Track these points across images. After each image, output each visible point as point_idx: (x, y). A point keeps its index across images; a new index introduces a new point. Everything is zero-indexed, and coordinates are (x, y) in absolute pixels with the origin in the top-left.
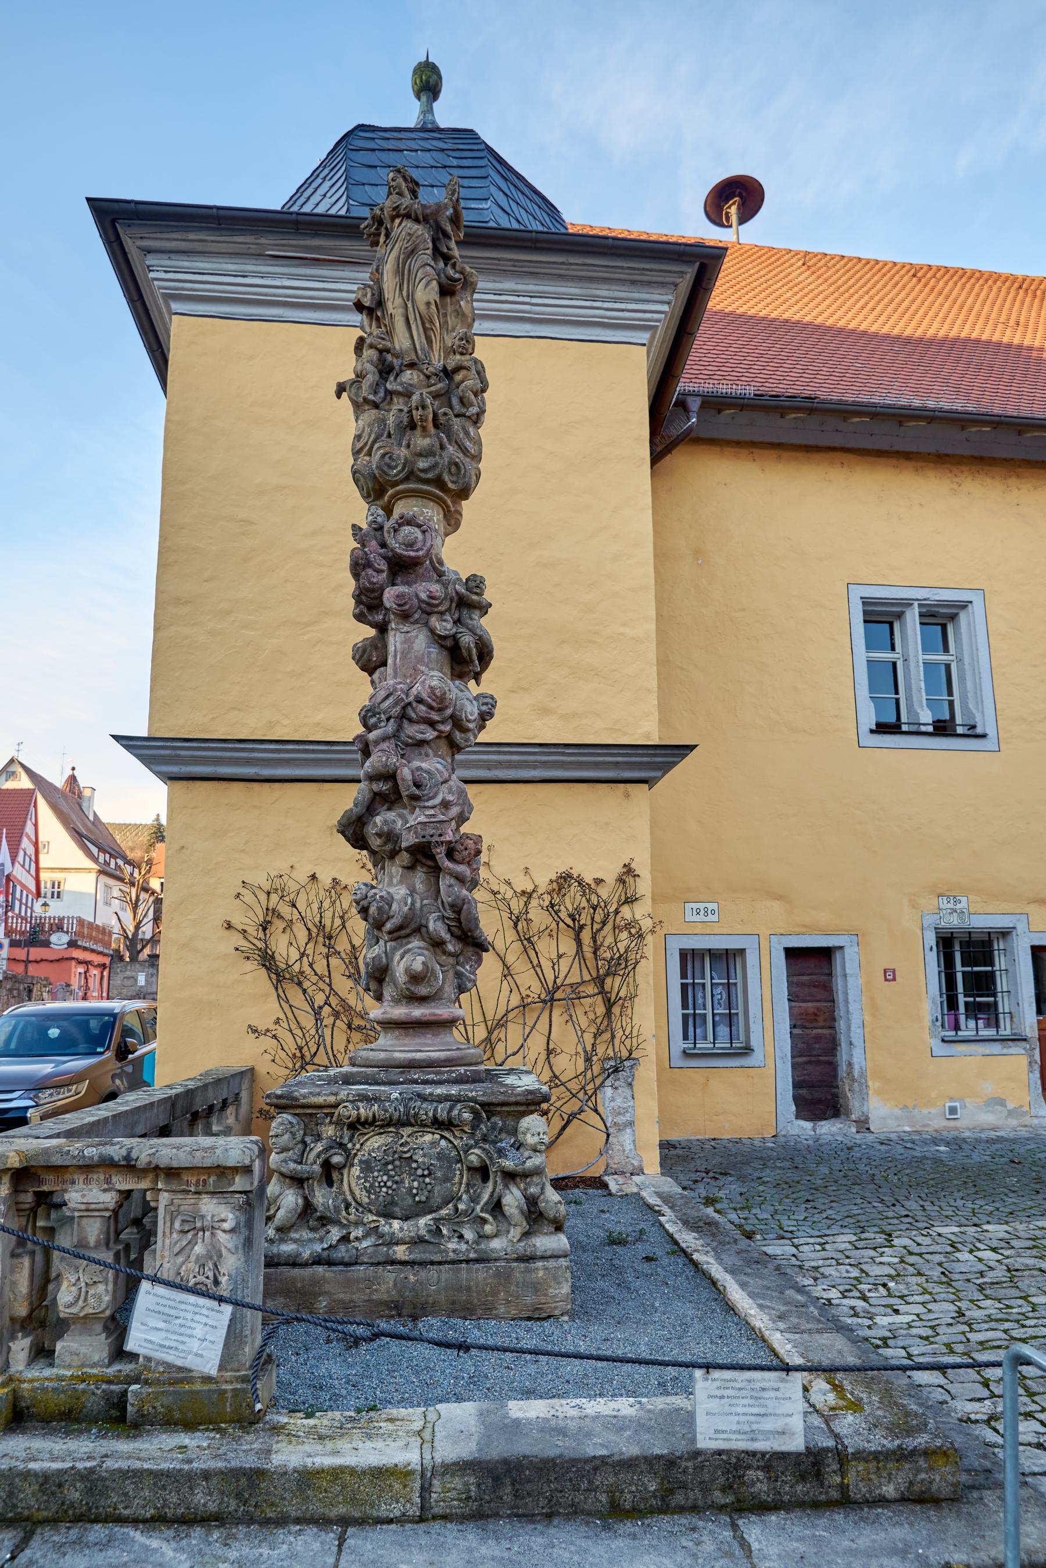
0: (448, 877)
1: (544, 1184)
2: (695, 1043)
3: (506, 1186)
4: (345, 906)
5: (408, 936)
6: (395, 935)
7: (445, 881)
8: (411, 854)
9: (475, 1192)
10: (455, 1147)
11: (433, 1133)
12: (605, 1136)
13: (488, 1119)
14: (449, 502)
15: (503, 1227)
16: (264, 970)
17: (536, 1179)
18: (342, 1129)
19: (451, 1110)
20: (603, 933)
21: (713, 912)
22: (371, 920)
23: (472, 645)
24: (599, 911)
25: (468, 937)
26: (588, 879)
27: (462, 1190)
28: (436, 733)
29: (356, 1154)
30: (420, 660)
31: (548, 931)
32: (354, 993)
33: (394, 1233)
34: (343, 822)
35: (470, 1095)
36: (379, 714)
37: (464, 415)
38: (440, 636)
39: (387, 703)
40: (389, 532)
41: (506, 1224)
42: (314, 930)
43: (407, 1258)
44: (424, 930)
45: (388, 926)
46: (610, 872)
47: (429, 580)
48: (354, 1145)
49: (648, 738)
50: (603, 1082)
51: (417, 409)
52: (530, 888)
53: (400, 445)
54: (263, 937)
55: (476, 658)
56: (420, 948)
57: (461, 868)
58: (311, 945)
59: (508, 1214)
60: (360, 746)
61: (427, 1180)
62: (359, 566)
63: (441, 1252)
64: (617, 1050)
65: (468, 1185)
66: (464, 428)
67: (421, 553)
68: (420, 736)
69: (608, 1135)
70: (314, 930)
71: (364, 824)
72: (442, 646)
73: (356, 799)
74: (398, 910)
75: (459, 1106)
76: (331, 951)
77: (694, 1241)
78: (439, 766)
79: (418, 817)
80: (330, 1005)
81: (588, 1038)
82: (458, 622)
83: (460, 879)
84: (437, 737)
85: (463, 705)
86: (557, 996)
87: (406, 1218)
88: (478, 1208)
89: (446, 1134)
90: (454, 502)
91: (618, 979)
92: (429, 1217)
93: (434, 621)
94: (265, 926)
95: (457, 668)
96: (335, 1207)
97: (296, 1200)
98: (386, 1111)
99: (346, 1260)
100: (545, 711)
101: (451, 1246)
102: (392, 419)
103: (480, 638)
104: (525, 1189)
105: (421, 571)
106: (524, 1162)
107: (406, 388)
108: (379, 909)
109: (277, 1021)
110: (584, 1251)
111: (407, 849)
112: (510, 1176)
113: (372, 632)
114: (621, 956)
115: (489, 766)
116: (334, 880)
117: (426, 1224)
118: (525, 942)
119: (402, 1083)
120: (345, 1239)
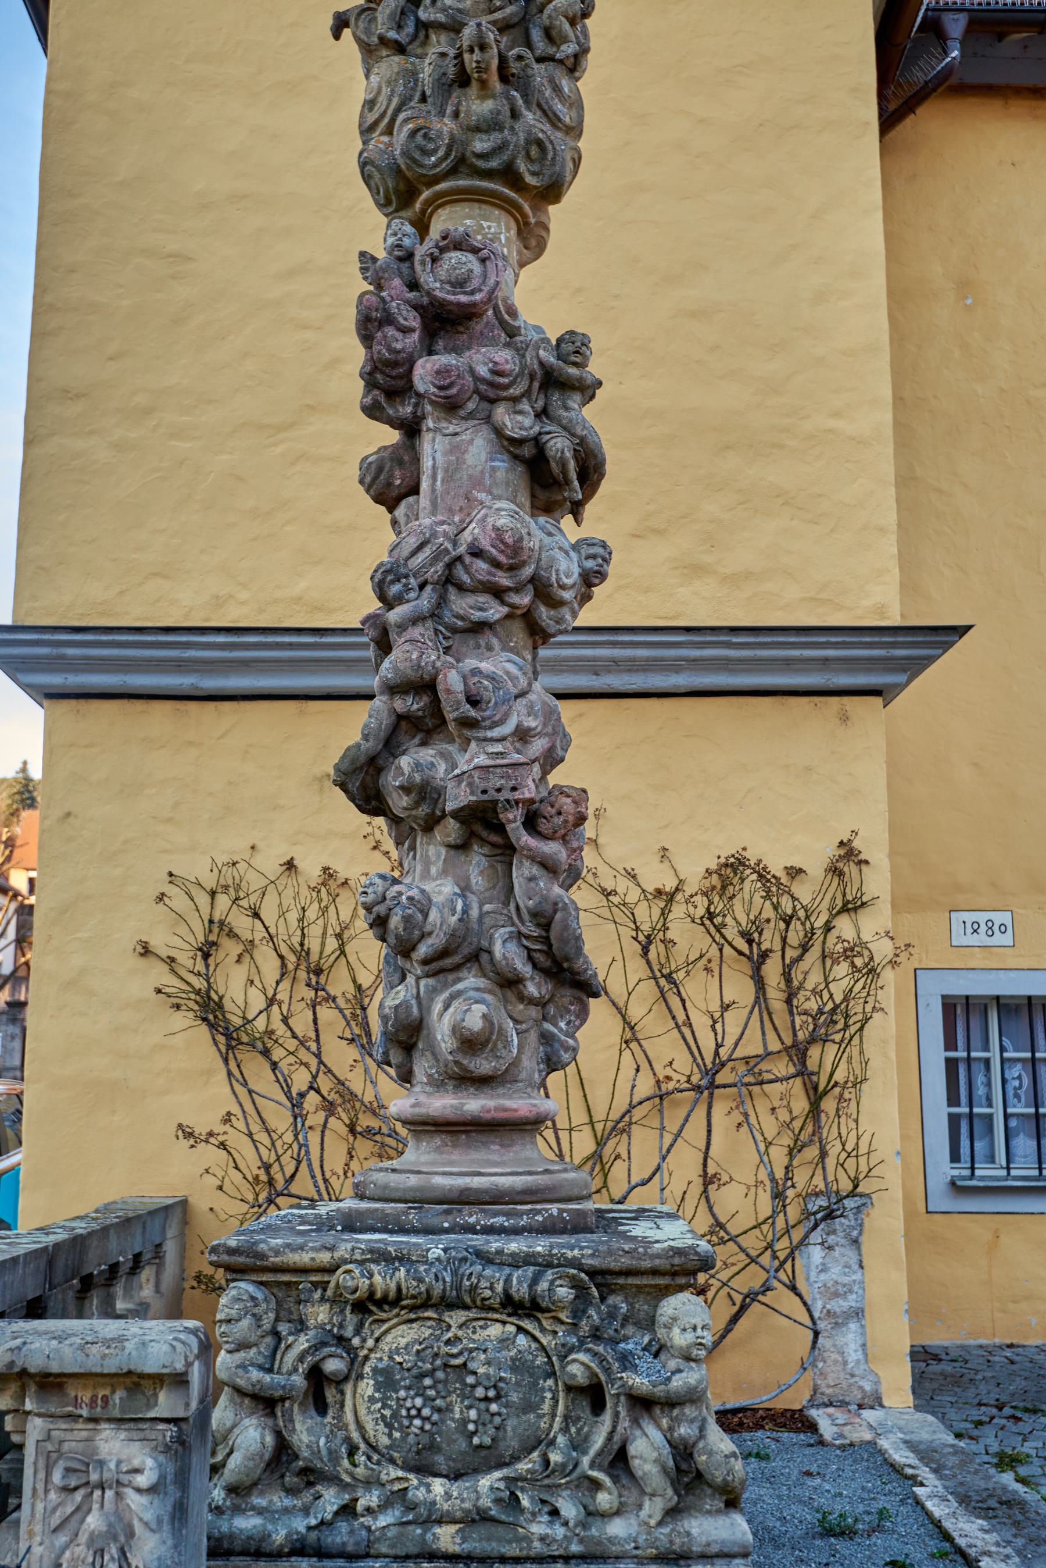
0: (527, 863)
1: (704, 1420)
2: (973, 1168)
3: (636, 1422)
4: (345, 915)
5: (457, 967)
6: (435, 966)
7: (522, 871)
8: (462, 823)
9: (579, 1431)
10: (543, 1348)
11: (504, 1323)
12: (810, 1335)
13: (603, 1299)
14: (527, 208)
15: (631, 1497)
16: (204, 1028)
17: (689, 1411)
18: (342, 1311)
19: (535, 1281)
20: (803, 965)
21: (1003, 929)
22: (392, 940)
23: (568, 454)
24: (795, 924)
25: (562, 970)
26: (776, 868)
27: (556, 1426)
28: (505, 610)
29: (366, 1358)
30: (477, 483)
31: (704, 961)
32: (359, 1069)
33: (434, 1503)
34: (344, 767)
35: (570, 1254)
36: (407, 577)
37: (551, 59)
38: (512, 441)
39: (420, 558)
40: (423, 263)
41: (635, 1492)
42: (291, 959)
43: (457, 1549)
44: (484, 957)
45: (423, 950)
46: (815, 855)
47: (494, 342)
48: (364, 1340)
49: (882, 615)
50: (806, 1236)
51: (471, 50)
52: (670, 885)
53: (442, 113)
54: (203, 971)
55: (573, 476)
56: (477, 989)
58: (285, 985)
59: (639, 1473)
60: (373, 633)
61: (494, 1407)
62: (371, 323)
63: (519, 1539)
64: (831, 1178)
65: (566, 1418)
66: (552, 81)
67: (478, 297)
68: (477, 615)
69: (816, 1334)
70: (291, 959)
71: (380, 770)
72: (516, 457)
73: (366, 726)
74: (440, 922)
75: (549, 1275)
76: (321, 996)
77: (980, 1534)
78: (510, 667)
79: (475, 756)
80: (318, 1091)
81: (779, 1156)
82: (543, 414)
83: (548, 866)
84: (508, 616)
85: (553, 559)
86: (720, 1079)
87: (455, 1476)
88: (586, 1461)
89: (527, 1324)
90: (535, 208)
91: (831, 1050)
92: (498, 1474)
94: (206, 952)
95: (542, 495)
96: (330, 1452)
97: (263, 1437)
98: (420, 1280)
99: (350, 1548)
100: (696, 570)
101: (537, 1529)
102: (428, 70)
103: (583, 441)
104: (671, 1429)
105: (478, 328)
106: (669, 1379)
107: (452, 17)
108: (407, 919)
109: (227, 1119)
110: (777, 1547)
111: (456, 815)
112: (643, 1404)
113: (392, 436)
114: (836, 1007)
115: (595, 668)
116: (326, 869)
117: (491, 1488)
118: (663, 982)
119: (447, 1231)
120: (348, 1510)
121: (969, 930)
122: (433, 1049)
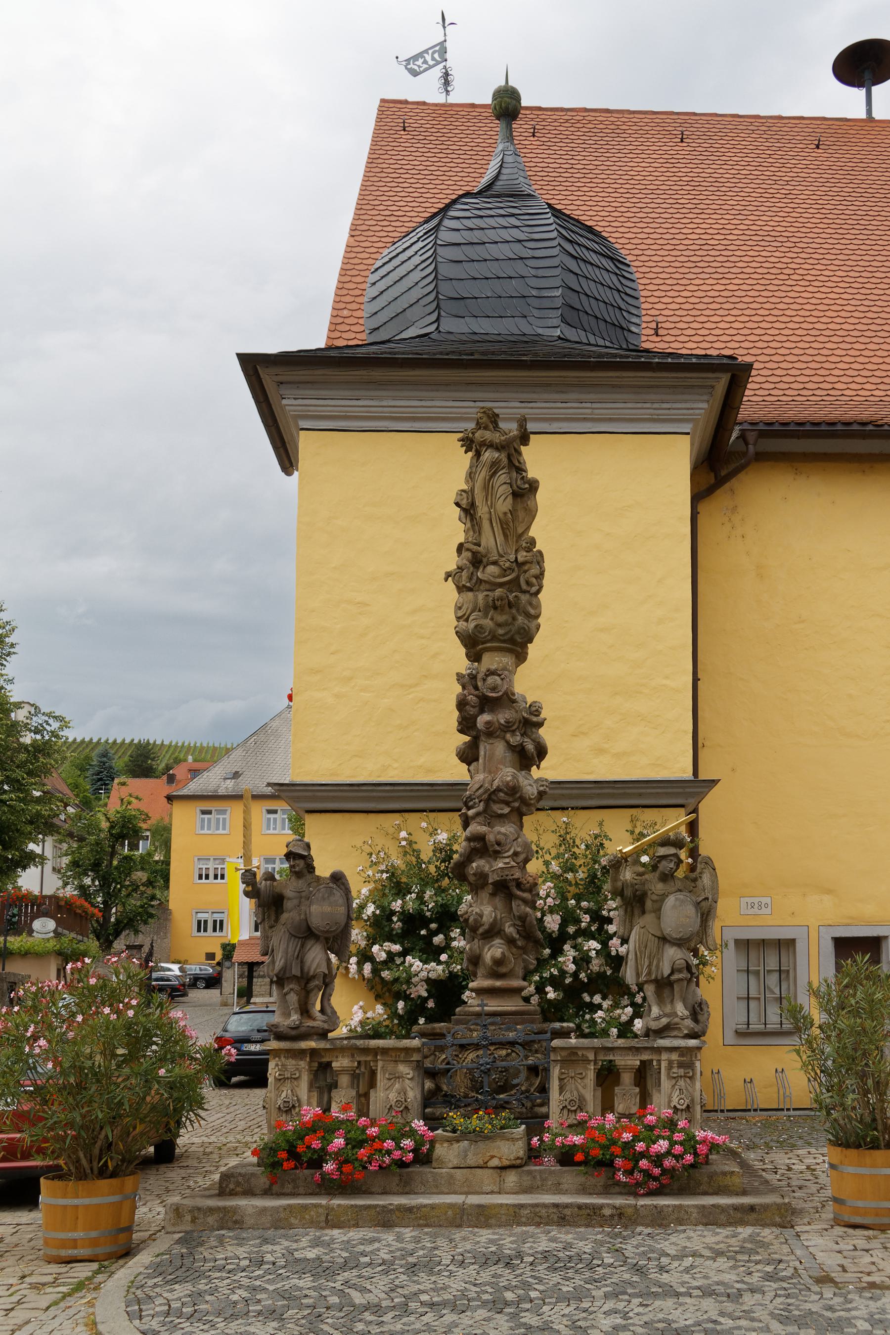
5: (492, 937)
45: (481, 930)
57: (526, 895)
71: (465, 867)
83: (525, 901)
93: (508, 736)
121: (749, 907)
122: (484, 964)
